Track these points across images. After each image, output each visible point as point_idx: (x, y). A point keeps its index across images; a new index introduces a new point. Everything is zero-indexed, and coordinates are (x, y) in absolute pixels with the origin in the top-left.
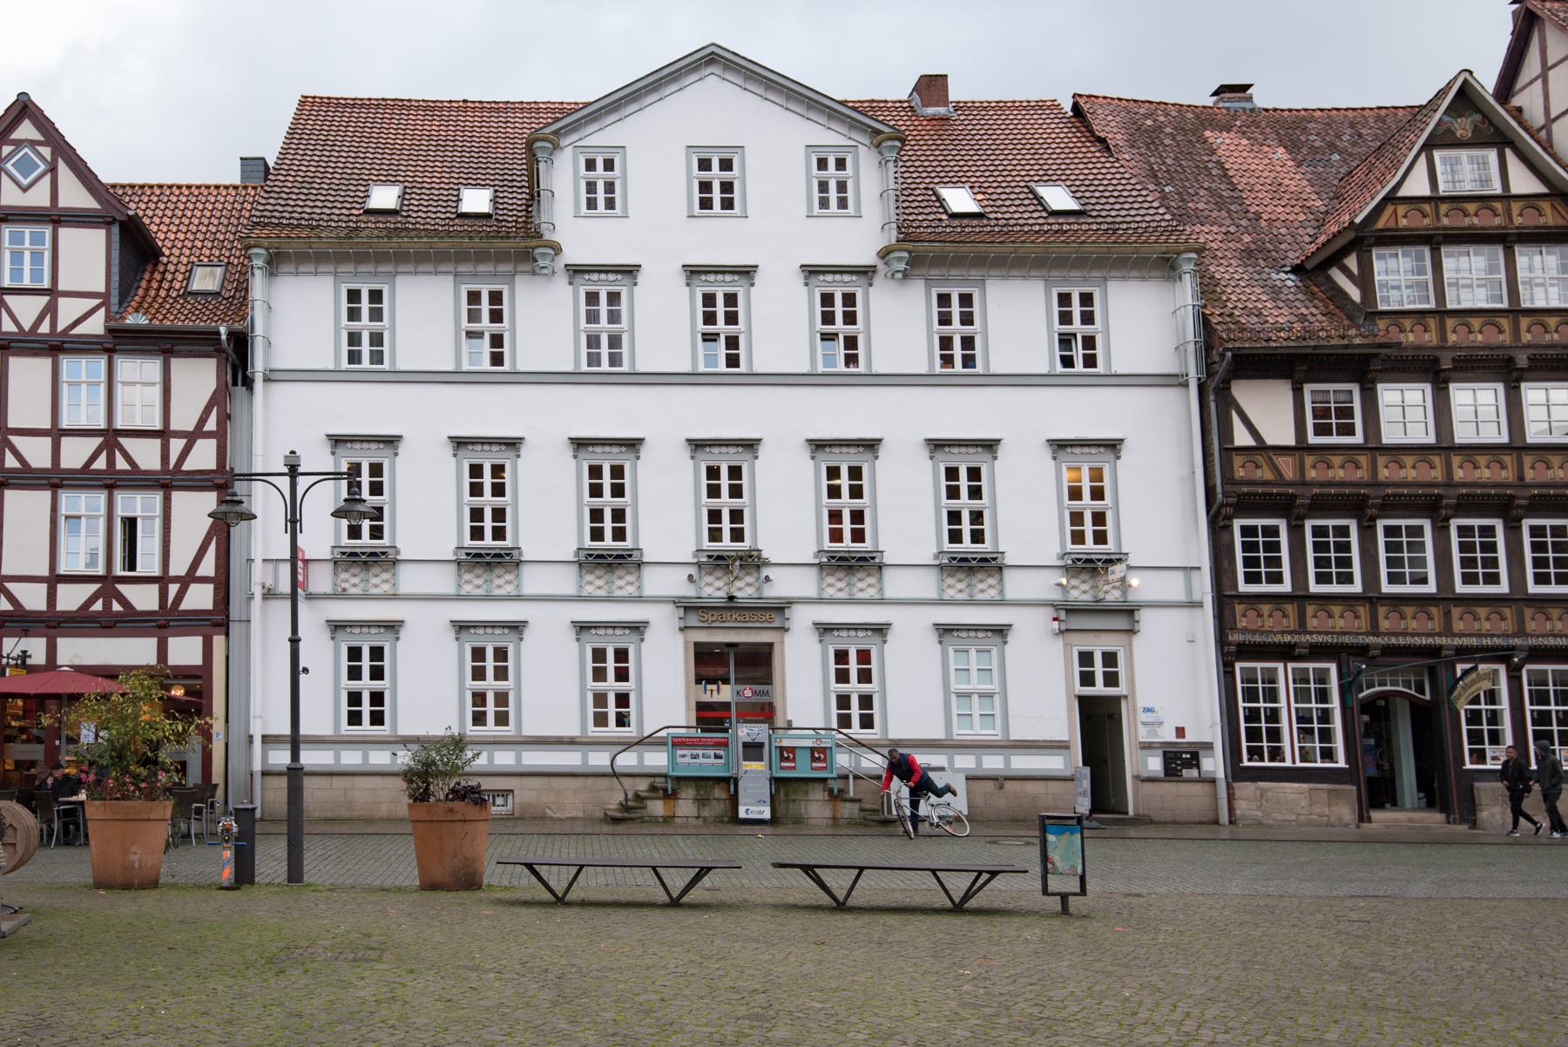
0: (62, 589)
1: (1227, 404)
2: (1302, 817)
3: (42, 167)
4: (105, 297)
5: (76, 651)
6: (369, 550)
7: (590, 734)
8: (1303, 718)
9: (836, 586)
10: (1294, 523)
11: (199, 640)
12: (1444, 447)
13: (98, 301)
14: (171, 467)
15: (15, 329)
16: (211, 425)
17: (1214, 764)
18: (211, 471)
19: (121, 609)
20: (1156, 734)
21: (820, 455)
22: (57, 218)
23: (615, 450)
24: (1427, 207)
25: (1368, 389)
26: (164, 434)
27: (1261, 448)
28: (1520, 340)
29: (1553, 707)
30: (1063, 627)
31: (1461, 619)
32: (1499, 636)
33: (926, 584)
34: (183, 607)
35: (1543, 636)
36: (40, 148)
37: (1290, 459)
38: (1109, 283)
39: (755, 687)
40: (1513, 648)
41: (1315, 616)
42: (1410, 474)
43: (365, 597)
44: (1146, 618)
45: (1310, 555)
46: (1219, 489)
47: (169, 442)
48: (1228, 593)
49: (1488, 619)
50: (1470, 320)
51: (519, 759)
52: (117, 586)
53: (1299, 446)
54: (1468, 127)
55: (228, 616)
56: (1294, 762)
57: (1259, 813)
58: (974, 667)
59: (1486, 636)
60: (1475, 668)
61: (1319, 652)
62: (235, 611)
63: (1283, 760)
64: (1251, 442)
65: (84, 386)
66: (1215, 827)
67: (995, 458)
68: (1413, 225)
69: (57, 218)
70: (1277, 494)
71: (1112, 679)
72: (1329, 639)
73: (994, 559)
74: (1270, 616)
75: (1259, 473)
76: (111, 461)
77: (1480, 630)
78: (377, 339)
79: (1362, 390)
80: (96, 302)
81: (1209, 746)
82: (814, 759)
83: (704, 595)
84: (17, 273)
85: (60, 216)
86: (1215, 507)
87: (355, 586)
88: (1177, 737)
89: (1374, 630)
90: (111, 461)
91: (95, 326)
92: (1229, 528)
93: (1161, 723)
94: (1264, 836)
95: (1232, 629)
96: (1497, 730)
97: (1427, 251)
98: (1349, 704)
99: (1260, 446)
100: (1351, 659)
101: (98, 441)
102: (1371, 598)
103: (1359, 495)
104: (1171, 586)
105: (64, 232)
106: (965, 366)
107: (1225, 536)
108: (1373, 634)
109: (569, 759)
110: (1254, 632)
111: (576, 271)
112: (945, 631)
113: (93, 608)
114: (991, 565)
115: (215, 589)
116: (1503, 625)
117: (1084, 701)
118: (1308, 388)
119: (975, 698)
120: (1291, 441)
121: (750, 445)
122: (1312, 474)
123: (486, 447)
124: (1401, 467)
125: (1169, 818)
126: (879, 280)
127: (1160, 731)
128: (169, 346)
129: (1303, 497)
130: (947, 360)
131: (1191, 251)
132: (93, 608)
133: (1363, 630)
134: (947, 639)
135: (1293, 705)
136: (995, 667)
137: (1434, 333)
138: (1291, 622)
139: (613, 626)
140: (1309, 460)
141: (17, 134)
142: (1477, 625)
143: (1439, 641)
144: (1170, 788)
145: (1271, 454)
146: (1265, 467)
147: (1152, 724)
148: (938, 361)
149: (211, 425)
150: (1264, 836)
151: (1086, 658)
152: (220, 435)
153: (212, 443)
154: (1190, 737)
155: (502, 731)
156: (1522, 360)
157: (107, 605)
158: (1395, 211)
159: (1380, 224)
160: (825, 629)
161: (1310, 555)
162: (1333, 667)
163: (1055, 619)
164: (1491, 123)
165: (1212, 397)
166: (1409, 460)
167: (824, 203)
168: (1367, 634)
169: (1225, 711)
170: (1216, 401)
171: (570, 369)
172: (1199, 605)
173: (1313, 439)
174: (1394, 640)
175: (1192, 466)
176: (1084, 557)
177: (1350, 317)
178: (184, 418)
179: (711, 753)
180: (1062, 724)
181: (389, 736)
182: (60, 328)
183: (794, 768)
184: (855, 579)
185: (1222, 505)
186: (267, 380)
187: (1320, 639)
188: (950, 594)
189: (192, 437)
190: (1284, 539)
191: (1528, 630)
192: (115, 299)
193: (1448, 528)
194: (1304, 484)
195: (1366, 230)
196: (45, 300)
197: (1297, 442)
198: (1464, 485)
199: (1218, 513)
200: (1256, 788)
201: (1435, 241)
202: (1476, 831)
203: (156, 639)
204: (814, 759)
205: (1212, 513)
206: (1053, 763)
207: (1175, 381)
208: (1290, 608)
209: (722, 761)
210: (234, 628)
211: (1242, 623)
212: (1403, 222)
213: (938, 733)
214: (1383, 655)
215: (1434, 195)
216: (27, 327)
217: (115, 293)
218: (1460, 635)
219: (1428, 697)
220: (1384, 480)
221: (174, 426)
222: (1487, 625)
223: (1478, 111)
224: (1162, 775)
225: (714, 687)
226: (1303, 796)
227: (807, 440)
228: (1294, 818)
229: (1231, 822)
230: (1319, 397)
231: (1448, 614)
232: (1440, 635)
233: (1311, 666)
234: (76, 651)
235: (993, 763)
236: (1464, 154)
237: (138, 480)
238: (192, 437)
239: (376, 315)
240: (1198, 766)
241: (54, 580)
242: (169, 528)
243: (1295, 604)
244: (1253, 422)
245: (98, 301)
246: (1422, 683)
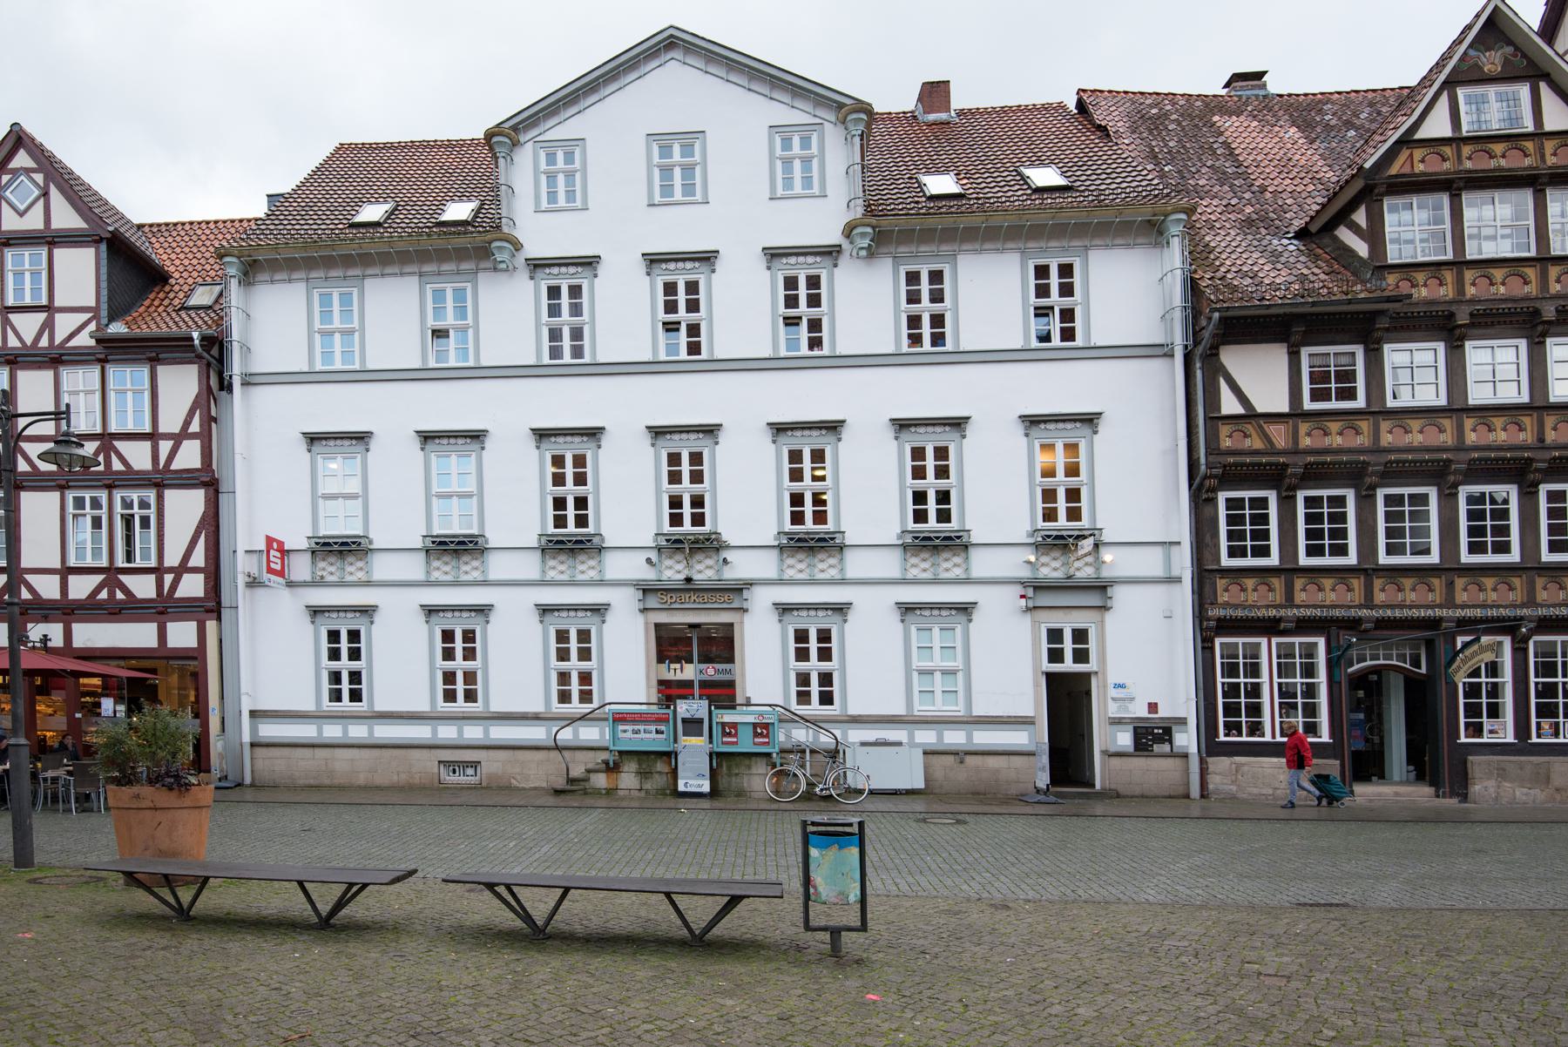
1: (1215, 370)
2: (1278, 792)
3: (37, 192)
4: (95, 311)
5: (89, 635)
7: (555, 710)
8: (1285, 692)
9: (797, 567)
10: (1284, 494)
11: (194, 624)
12: (1457, 409)
14: (161, 467)
15: (19, 345)
16: (195, 427)
17: (1187, 739)
18: (197, 470)
19: (124, 597)
20: (1127, 711)
21: (661, 442)
22: (52, 239)
23: (577, 439)
24: (1447, 150)
25: (1373, 350)
26: (153, 437)
27: (1251, 416)
28: (1548, 292)
29: (1242, 680)
30: (1031, 604)
31: (1465, 590)
32: (1505, 607)
33: (529, 566)
34: (178, 594)
35: (1554, 606)
36: (34, 175)
37: (1282, 427)
38: (366, 281)
39: (718, 666)
40: (1522, 618)
41: (1304, 590)
42: (1417, 439)
43: (342, 584)
44: (1120, 594)
45: (1301, 527)
46: (1203, 460)
47: (158, 444)
48: (1210, 567)
49: (1495, 589)
50: (1492, 271)
51: (371, 732)
52: (120, 576)
53: (1292, 412)
54: (1497, 61)
55: (219, 603)
56: (1274, 736)
57: (1234, 788)
58: (937, 644)
59: (1491, 607)
60: (1477, 640)
61: (1305, 626)
62: (225, 601)
63: (1263, 735)
64: (1239, 409)
65: (82, 394)
66: (1186, 800)
67: (964, 437)
68: (1430, 170)
69: (52, 239)
70: (1250, 464)
71: (1081, 656)
72: (1318, 612)
73: (959, 537)
74: (1255, 590)
75: (1248, 443)
77: (1405, 601)
79: (1367, 351)
80: (89, 315)
81: (1182, 722)
82: (756, 735)
83: (664, 578)
84: (19, 291)
85: (54, 237)
86: (1198, 481)
87: (332, 574)
88: (1149, 713)
89: (1369, 603)
92: (1213, 501)
93: (1132, 699)
95: (1212, 604)
96: (1497, 703)
97: (1445, 199)
98: (1337, 678)
99: (1250, 413)
100: (1342, 633)
102: (1365, 570)
103: (1358, 462)
104: (1149, 563)
105: (59, 253)
106: (934, 344)
107: (1208, 510)
108: (1367, 607)
109: (420, 732)
110: (1236, 607)
111: (537, 266)
112: (907, 610)
113: (99, 597)
114: (956, 544)
115: (206, 578)
116: (1511, 596)
117: (1050, 677)
118: (1305, 352)
119: (938, 675)
120: (1284, 408)
121: (710, 431)
122: (1306, 442)
123: (452, 441)
124: (1407, 432)
125: (1138, 791)
126: (844, 261)
127: (1131, 706)
128: (154, 354)
129: (1295, 465)
130: (916, 340)
131: (1180, 212)
132: (99, 597)
133: (1357, 603)
134: (910, 617)
135: (1276, 680)
136: (959, 644)
137: (1450, 286)
138: (1278, 596)
139: (575, 608)
140: (1304, 427)
141: (14, 164)
142: (1482, 596)
143: (1438, 613)
144: (1139, 763)
145: (1262, 422)
146: (1254, 435)
147: (1123, 700)
148: (905, 341)
151: (1055, 635)
152: (205, 437)
153: (197, 443)
154: (1163, 712)
155: (470, 707)
156: (1549, 312)
157: (112, 594)
158: (1411, 155)
159: (1394, 170)
160: (784, 609)
161: (1301, 527)
162: (1321, 642)
163: (1022, 597)
164: (1524, 56)
165: (1198, 365)
166: (1415, 424)
167: (667, 190)
168: (1360, 607)
169: (1201, 685)
170: (1202, 368)
171: (532, 362)
172: (1178, 580)
173: (1308, 405)
174: (1389, 613)
175: (1176, 439)
176: (1055, 533)
177: (1354, 274)
178: (171, 422)
179: (653, 728)
180: (1030, 700)
181: (365, 712)
182: (57, 342)
183: (736, 743)
184: (816, 560)
185: (1205, 477)
187: (1308, 612)
188: (913, 573)
189: (178, 438)
190: (1273, 511)
191: (1539, 600)
192: (104, 313)
194: (1296, 452)
195: (1377, 177)
196: (42, 316)
197: (1291, 408)
198: (1476, 448)
199: (1201, 485)
200: (1231, 763)
201: (1455, 186)
202: (1466, 805)
203: (156, 624)
204: (756, 735)
205: (1193, 487)
206: (1017, 738)
207: (1161, 351)
208: (1277, 583)
209: (664, 736)
210: (225, 614)
211: (1223, 597)
212: (1420, 168)
213: (899, 709)
214: (1376, 628)
215: (1457, 135)
217: (104, 306)
218: (1463, 607)
219: (1423, 670)
220: (1386, 445)
221: (162, 429)
222: (1494, 596)
223: (1510, 42)
224: (1131, 749)
225: (678, 666)
226: (1281, 771)
227: (647, 427)
228: (1271, 792)
229: (1202, 796)
230: (1318, 361)
231: (1451, 584)
232: (1440, 606)
233: (1297, 640)
234: (89, 635)
235: (955, 738)
236: (1491, 91)
237: (133, 479)
238: (178, 438)
240: (1171, 742)
241: (66, 572)
242: (163, 524)
243: (1283, 577)
244: (1243, 390)
246: (1419, 656)
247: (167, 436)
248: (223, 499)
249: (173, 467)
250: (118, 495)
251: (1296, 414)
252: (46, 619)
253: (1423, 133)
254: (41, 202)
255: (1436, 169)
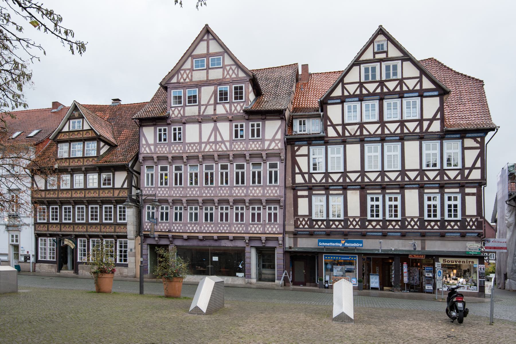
17: (32, 259)
24: (68, 134)
94: (43, 276)
108: (60, 231)
127: (24, 252)
150: (43, 276)
187: (52, 233)
193: (62, 207)
201: (70, 141)
251: (46, 190)
253: (64, 130)
255: (65, 138)
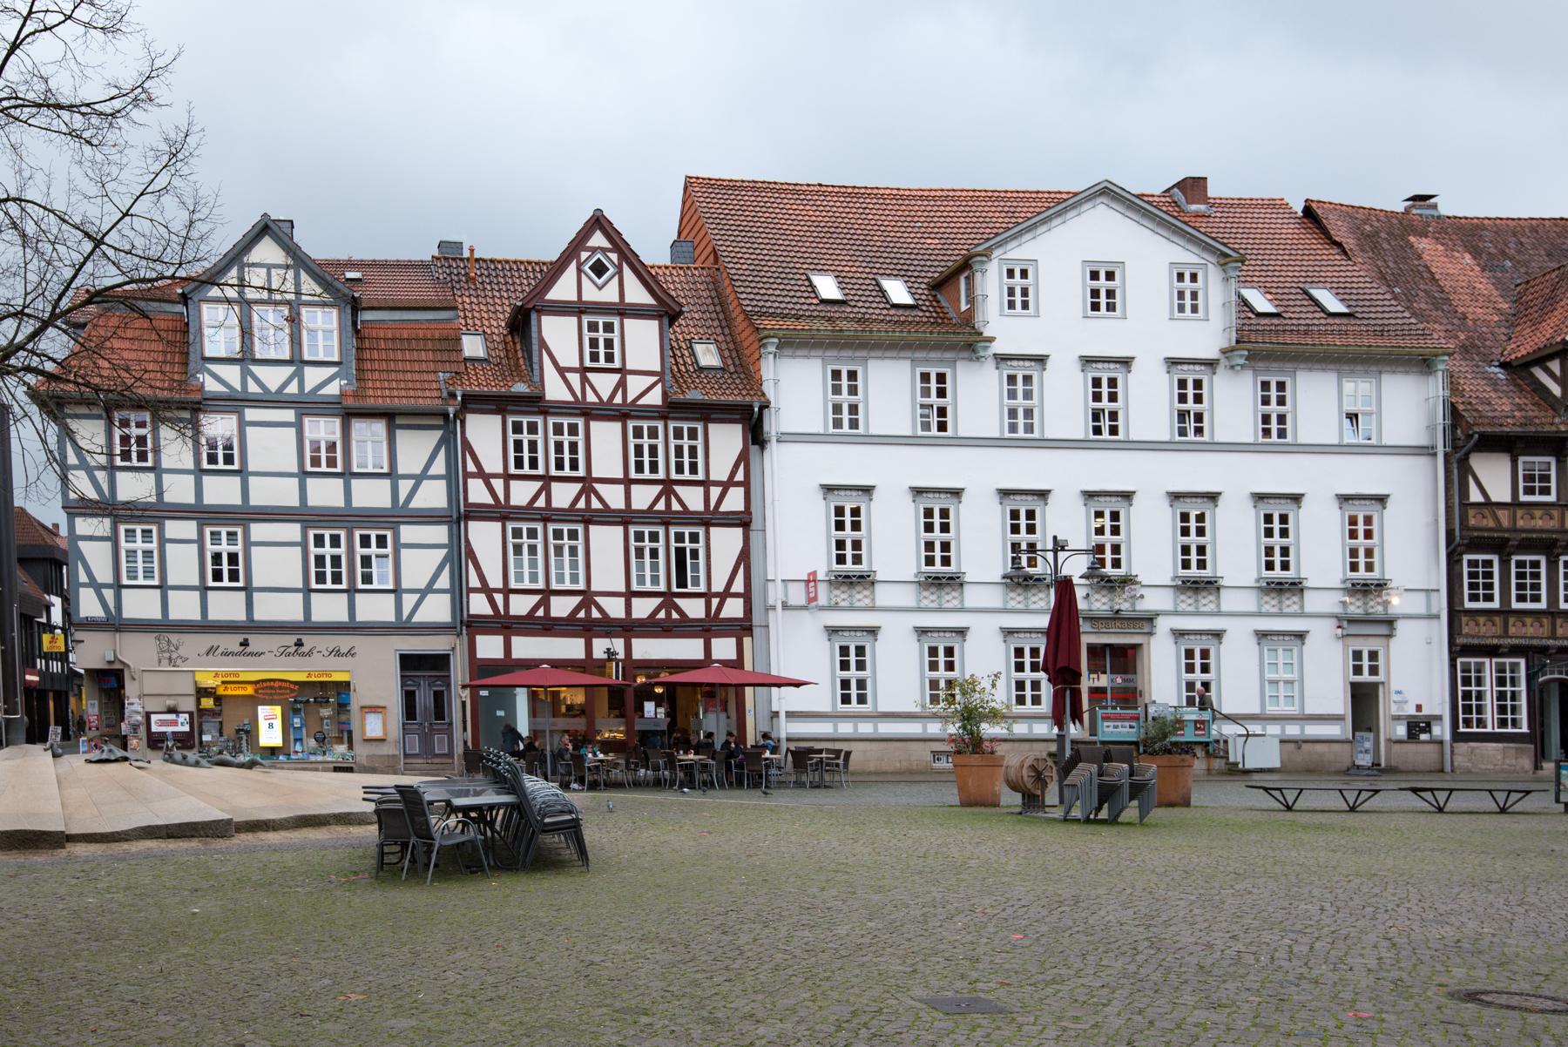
0: (635, 601)
4: (660, 375)
6: (858, 574)
11: (733, 641)
13: (655, 379)
16: (740, 476)
18: (741, 512)
34: (722, 615)
36: (609, 254)
62: (757, 619)
76: (668, 504)
78: (854, 409)
80: (655, 379)
90: (668, 504)
91: (655, 398)
101: (659, 488)
149: (740, 476)
153: (741, 490)
157: (668, 614)
182: (630, 399)
186: (778, 441)
189: (726, 485)
192: (668, 377)
196: (617, 377)
210: (756, 631)
216: (605, 398)
221: (712, 478)
238: (726, 485)
239: (853, 390)
245: (655, 379)
247: (717, 483)
248: (753, 535)
249: (722, 509)
250: (673, 530)
252: (608, 635)
254: (616, 278)
